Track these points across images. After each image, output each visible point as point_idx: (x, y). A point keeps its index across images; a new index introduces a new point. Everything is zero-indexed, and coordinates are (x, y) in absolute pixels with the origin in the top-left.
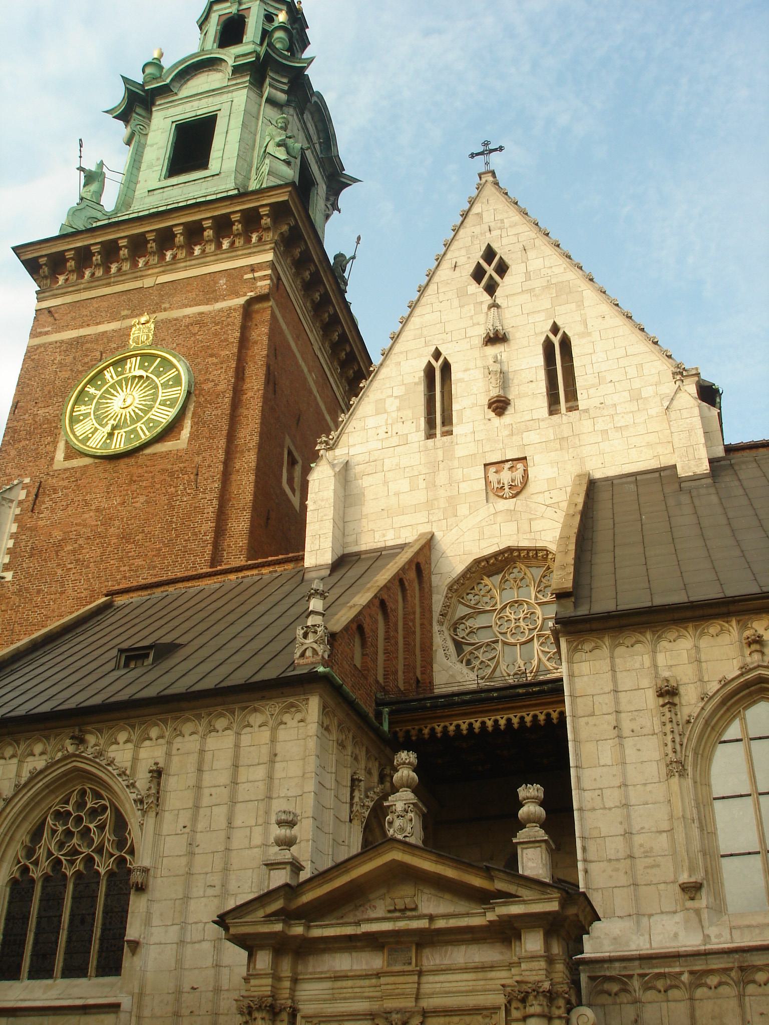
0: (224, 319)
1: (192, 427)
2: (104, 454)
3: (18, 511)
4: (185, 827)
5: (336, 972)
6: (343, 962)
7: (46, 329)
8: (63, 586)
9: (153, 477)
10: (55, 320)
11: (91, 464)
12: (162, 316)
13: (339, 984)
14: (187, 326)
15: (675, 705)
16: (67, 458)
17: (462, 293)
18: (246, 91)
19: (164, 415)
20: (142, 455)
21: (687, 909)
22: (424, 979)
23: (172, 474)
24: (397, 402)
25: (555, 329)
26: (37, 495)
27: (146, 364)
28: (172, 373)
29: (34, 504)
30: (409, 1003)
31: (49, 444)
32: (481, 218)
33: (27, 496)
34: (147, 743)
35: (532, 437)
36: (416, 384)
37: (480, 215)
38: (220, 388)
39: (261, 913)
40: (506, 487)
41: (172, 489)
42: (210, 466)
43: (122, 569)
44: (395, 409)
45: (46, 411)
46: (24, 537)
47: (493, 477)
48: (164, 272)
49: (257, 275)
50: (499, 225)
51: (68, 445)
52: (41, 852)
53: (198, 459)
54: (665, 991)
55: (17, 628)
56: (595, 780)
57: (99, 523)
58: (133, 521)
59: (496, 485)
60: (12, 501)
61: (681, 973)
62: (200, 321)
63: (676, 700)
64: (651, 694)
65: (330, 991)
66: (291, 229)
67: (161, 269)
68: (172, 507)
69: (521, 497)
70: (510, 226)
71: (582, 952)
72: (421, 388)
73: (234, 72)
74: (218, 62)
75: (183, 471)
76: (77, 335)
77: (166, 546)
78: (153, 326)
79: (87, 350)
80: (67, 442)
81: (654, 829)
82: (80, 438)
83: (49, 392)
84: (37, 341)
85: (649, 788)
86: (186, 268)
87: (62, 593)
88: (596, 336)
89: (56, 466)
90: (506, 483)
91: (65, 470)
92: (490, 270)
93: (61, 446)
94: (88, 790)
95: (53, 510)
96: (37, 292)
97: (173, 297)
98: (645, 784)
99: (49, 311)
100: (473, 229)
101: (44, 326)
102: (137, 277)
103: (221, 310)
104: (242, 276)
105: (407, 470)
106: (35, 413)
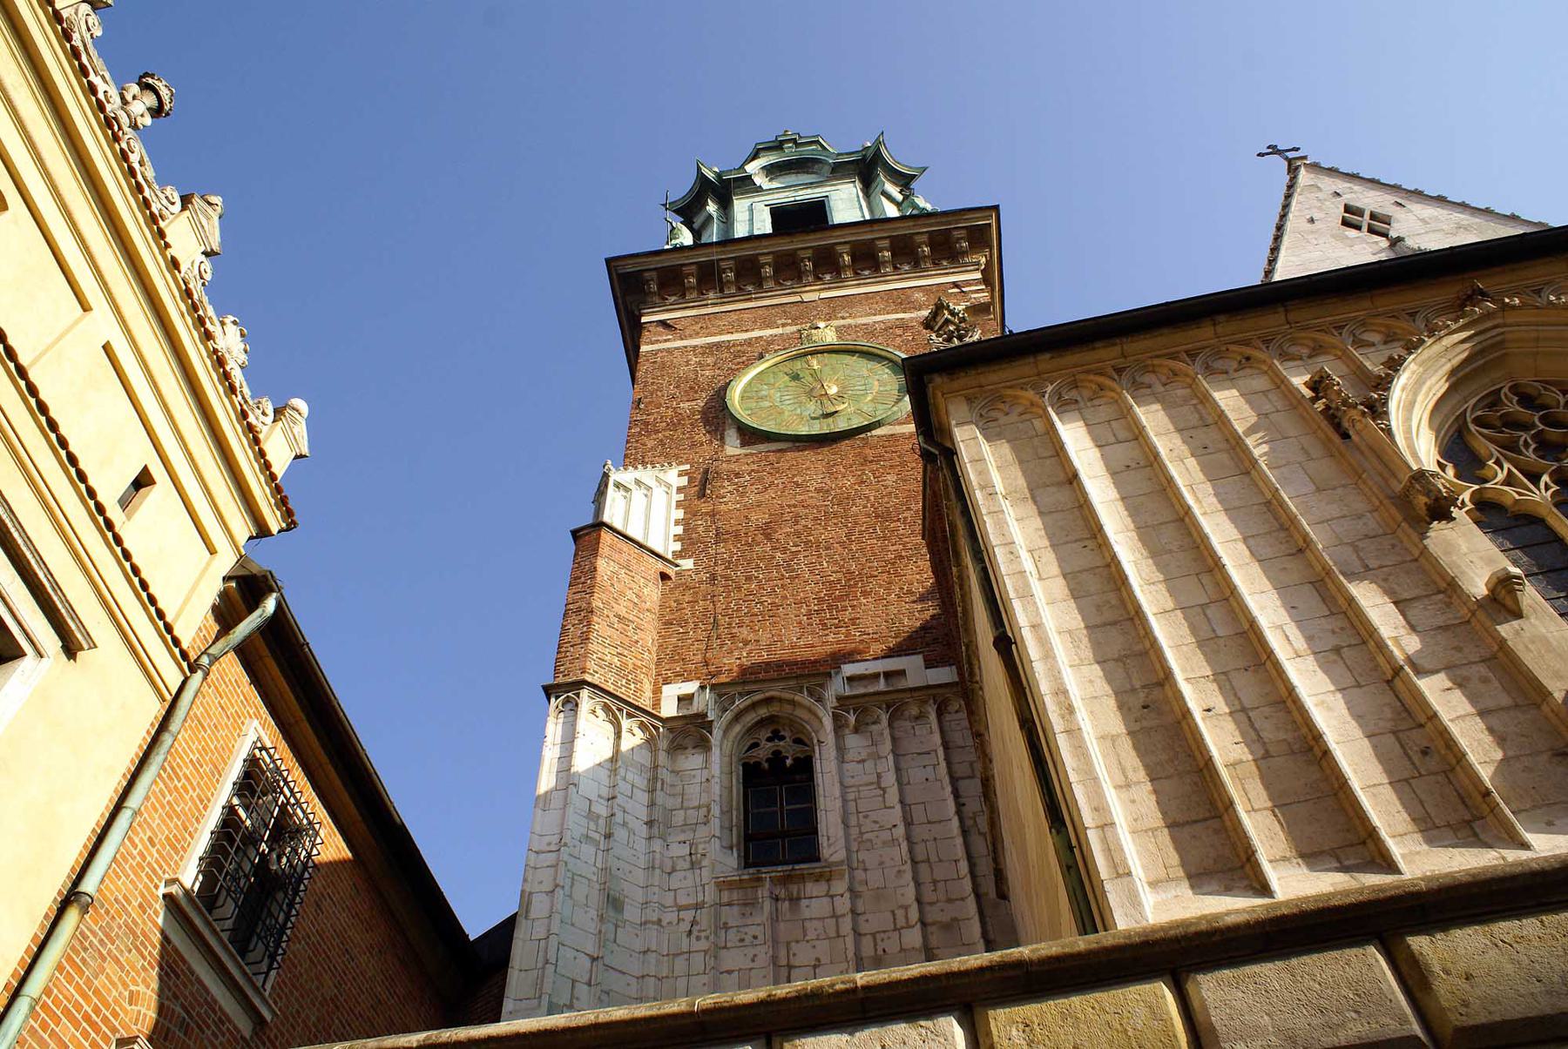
3: (681, 497)
55: (723, 621)
74: (810, 164)
95: (742, 495)
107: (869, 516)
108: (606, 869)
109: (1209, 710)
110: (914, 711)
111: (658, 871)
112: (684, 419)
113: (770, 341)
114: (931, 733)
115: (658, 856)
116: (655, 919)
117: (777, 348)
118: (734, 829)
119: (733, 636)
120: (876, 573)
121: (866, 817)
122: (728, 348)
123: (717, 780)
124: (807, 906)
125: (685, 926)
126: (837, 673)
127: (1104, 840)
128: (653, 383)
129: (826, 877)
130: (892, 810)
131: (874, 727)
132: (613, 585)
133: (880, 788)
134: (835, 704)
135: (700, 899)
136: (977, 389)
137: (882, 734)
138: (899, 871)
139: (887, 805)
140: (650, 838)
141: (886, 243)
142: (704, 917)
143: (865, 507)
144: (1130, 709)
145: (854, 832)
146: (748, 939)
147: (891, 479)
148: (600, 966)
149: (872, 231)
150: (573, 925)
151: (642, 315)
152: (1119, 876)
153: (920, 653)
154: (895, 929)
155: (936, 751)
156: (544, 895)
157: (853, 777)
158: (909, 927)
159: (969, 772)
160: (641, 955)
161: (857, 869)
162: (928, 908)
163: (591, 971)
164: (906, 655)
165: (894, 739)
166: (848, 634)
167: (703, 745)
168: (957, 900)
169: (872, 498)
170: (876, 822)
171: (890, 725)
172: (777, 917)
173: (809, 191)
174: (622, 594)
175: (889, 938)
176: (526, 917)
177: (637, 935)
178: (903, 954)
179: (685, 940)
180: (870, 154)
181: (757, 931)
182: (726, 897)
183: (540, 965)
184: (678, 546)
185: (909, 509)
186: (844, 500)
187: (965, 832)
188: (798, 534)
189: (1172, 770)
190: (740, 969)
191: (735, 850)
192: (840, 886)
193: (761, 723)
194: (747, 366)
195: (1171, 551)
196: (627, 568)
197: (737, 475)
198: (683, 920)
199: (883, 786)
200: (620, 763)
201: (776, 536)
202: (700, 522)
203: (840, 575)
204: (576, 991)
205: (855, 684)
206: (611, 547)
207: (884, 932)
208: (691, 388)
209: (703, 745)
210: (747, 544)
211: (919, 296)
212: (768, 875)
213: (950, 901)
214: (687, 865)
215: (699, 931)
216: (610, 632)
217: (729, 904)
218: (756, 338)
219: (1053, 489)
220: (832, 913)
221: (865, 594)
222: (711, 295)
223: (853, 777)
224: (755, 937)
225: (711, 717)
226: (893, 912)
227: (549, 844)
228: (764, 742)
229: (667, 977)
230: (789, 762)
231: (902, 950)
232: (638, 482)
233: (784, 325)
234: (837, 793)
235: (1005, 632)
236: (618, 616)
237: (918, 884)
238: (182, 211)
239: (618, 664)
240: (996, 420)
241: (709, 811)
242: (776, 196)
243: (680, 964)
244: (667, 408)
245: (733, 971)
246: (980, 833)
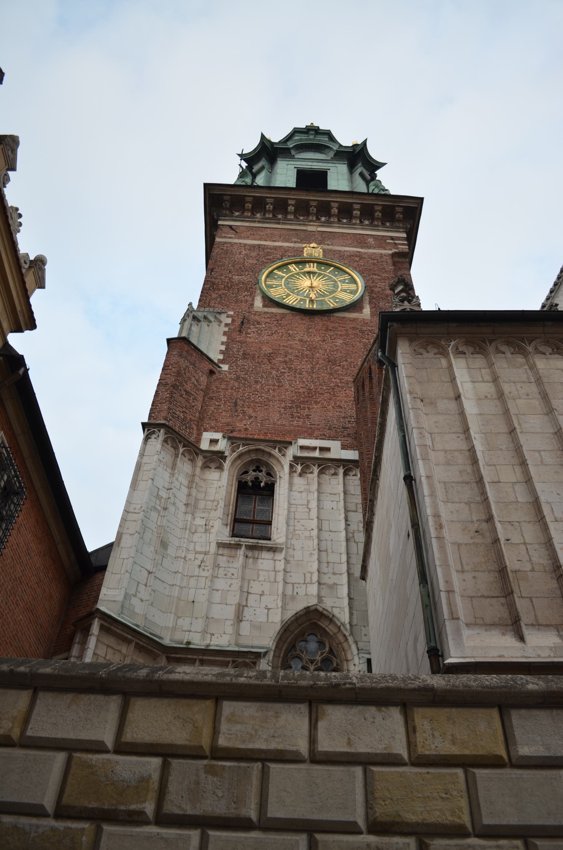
1: (371, 309)
3: (226, 329)
7: (230, 236)
10: (237, 232)
11: (289, 313)
12: (326, 247)
16: (264, 306)
20: (333, 316)
23: (362, 332)
27: (323, 268)
28: (347, 277)
31: (246, 295)
41: (365, 340)
55: (240, 403)
57: (305, 349)
58: (335, 353)
60: (220, 322)
67: (320, 224)
73: (335, 155)
79: (269, 252)
91: (265, 313)
95: (259, 335)
102: (301, 224)
106: (230, 277)
107: (324, 360)
108: (162, 526)
109: (508, 540)
110: (332, 471)
111: (188, 531)
112: (234, 285)
113: (287, 250)
114: (339, 484)
115: (189, 523)
116: (183, 556)
117: (290, 254)
118: (230, 516)
119: (244, 412)
120: (323, 392)
121: (299, 522)
122: (263, 249)
123: (225, 488)
124: (262, 563)
125: (198, 562)
126: (295, 443)
127: (448, 598)
128: (220, 261)
129: (273, 550)
130: (312, 521)
131: (309, 476)
132: (185, 373)
133: (308, 508)
134: (291, 459)
135: (207, 550)
136: (415, 335)
137: (313, 480)
138: (311, 554)
139: (310, 518)
140: (186, 513)
141: (358, 206)
142: (209, 560)
143: (324, 355)
144: (469, 531)
145: (291, 528)
146: (229, 575)
147: (339, 342)
148: (153, 578)
149: (352, 198)
150: (141, 553)
151: (220, 220)
152: (453, 619)
153: (340, 440)
154: (304, 583)
155: (339, 494)
156: (129, 535)
157: (295, 499)
158: (311, 583)
159: (355, 509)
160: (174, 574)
161: (290, 548)
162: (322, 575)
163: (148, 578)
164: (332, 440)
165: (319, 484)
166: (304, 423)
167: (220, 468)
168: (338, 574)
169: (328, 351)
170: (303, 526)
171: (319, 476)
172: (245, 567)
173: (320, 164)
174: (190, 379)
175: (300, 587)
176: (118, 546)
177: (173, 563)
178: (306, 597)
179: (197, 570)
180: (358, 149)
181: (232, 571)
182: (221, 552)
183: (122, 572)
184: (221, 357)
185: (346, 361)
186: (313, 349)
187: (347, 540)
188: (285, 362)
189: (485, 568)
190: (223, 590)
191: (229, 526)
192: (280, 556)
193: (252, 462)
194: (273, 262)
195: (501, 449)
196: (194, 364)
197: (258, 323)
198: (197, 559)
199: (310, 507)
200: (176, 471)
201: (274, 361)
202: (235, 346)
203: (304, 390)
204: (139, 588)
205: (303, 450)
206: (187, 351)
207: (299, 584)
208: (240, 268)
209: (220, 468)
210: (258, 363)
211: (371, 240)
212: (244, 544)
213: (334, 574)
214: (203, 530)
215: (205, 566)
216: (180, 399)
217: (222, 555)
218: (280, 247)
219: (446, 401)
220: (273, 569)
221: (317, 403)
222: (258, 215)
223: (295, 499)
224: (233, 574)
225: (227, 454)
226: (305, 574)
227: (135, 509)
228: (251, 471)
229: (185, 587)
230: (262, 484)
231: (306, 594)
232: (205, 318)
233: (295, 242)
234: (286, 507)
235: (410, 473)
236: (186, 391)
237: (319, 562)
238: (366, 582)
239: (183, 417)
240: (422, 354)
241: (218, 504)
242: (301, 163)
243: (193, 582)
244: (226, 277)
245: (219, 590)
246: (355, 542)
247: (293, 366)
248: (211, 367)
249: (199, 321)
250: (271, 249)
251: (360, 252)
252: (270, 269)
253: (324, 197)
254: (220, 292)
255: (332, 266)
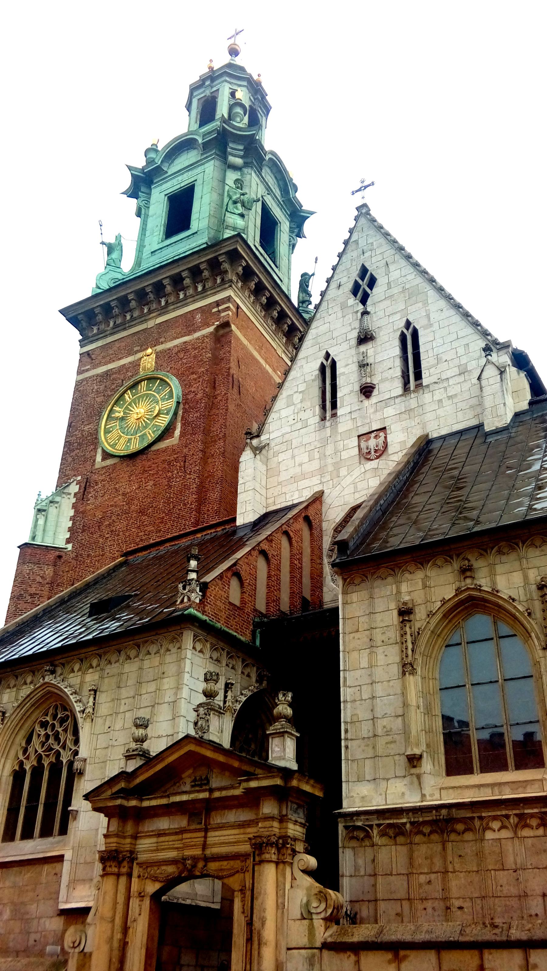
0: (200, 344)
2: (126, 454)
3: (74, 500)
4: (109, 728)
5: (160, 830)
6: (163, 824)
7: (87, 367)
8: (103, 550)
9: (157, 467)
12: (159, 348)
13: (162, 839)
14: (176, 353)
15: (410, 621)
16: (103, 459)
17: (344, 306)
18: (212, 162)
19: (164, 421)
21: (411, 775)
22: (210, 834)
24: (300, 396)
25: (408, 324)
26: (85, 488)
27: (151, 385)
29: (84, 494)
30: (198, 852)
31: (92, 450)
32: (358, 244)
33: (80, 489)
34: (91, 670)
35: (390, 411)
36: (313, 380)
37: (356, 242)
38: (199, 396)
39: (109, 793)
40: (373, 453)
42: (193, 454)
43: (140, 534)
44: (299, 401)
45: (90, 427)
46: (78, 519)
47: (363, 445)
48: (160, 315)
49: (220, 308)
50: (370, 248)
51: (104, 451)
52: (30, 750)
53: (185, 450)
54: (395, 837)
56: (357, 679)
57: (125, 503)
59: (366, 451)
60: (70, 494)
61: (405, 824)
62: (184, 349)
63: (412, 617)
64: (395, 613)
65: (155, 845)
66: (244, 268)
68: (170, 487)
69: (383, 457)
70: (378, 247)
71: (341, 807)
72: (317, 384)
75: (176, 460)
76: (106, 370)
77: (167, 515)
78: (154, 356)
79: (114, 379)
80: (103, 449)
81: (393, 714)
82: (111, 444)
83: (91, 413)
84: (81, 377)
85: (391, 683)
86: (174, 310)
87: (103, 555)
88: (436, 326)
89: (97, 466)
90: (372, 448)
91: (103, 468)
92: (364, 285)
93: (99, 451)
94: (59, 706)
96: (80, 341)
97: (167, 333)
98: (389, 681)
99: (88, 354)
100: (352, 254)
101: (85, 366)
103: (198, 339)
104: (211, 311)
105: (307, 446)
174: (34, 580)
247: (114, 528)
248: (57, 553)
249: (44, 511)
250: (116, 373)
251: (186, 342)
252: (109, 408)
253: (155, 277)
254: (73, 454)
255: (158, 378)
